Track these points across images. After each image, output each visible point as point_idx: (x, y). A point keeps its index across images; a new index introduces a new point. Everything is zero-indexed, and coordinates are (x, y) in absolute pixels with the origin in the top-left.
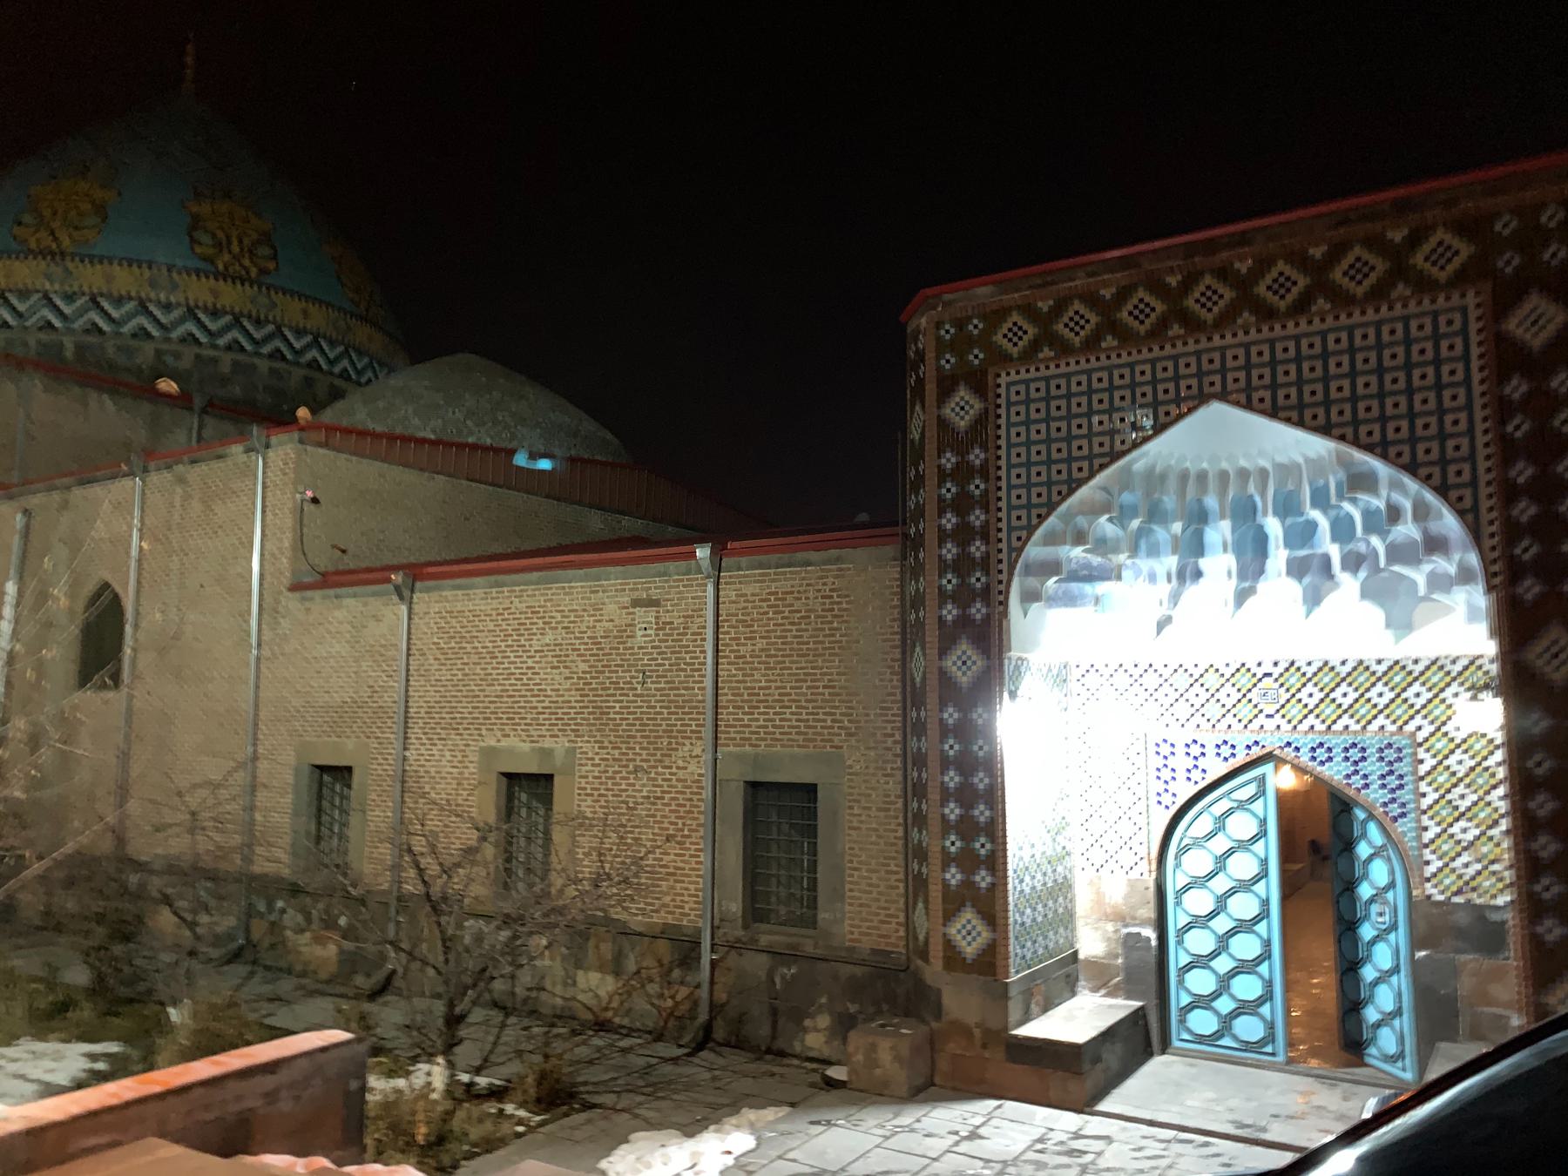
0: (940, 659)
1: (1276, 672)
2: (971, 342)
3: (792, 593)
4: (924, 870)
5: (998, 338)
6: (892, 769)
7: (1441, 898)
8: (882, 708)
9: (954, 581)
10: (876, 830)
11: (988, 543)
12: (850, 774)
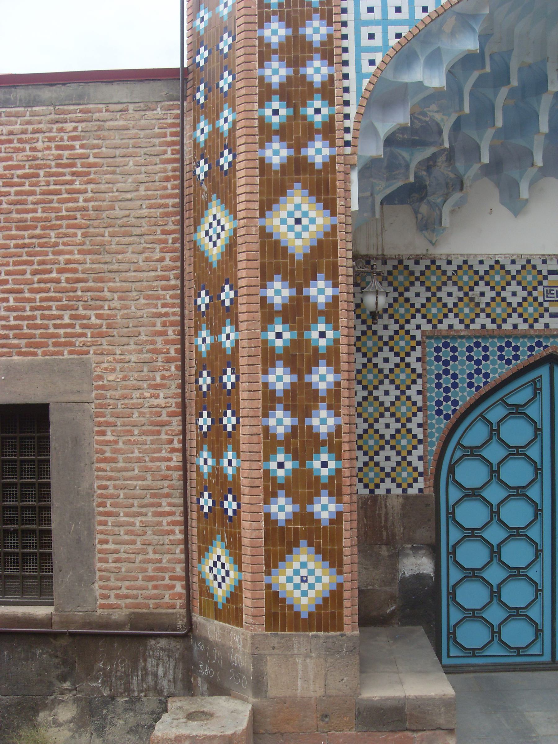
0: (262, 215)
3: (10, 141)
4: (230, 505)
8: (147, 297)
9: (283, 112)
10: (139, 460)
11: (331, 63)
12: (98, 388)
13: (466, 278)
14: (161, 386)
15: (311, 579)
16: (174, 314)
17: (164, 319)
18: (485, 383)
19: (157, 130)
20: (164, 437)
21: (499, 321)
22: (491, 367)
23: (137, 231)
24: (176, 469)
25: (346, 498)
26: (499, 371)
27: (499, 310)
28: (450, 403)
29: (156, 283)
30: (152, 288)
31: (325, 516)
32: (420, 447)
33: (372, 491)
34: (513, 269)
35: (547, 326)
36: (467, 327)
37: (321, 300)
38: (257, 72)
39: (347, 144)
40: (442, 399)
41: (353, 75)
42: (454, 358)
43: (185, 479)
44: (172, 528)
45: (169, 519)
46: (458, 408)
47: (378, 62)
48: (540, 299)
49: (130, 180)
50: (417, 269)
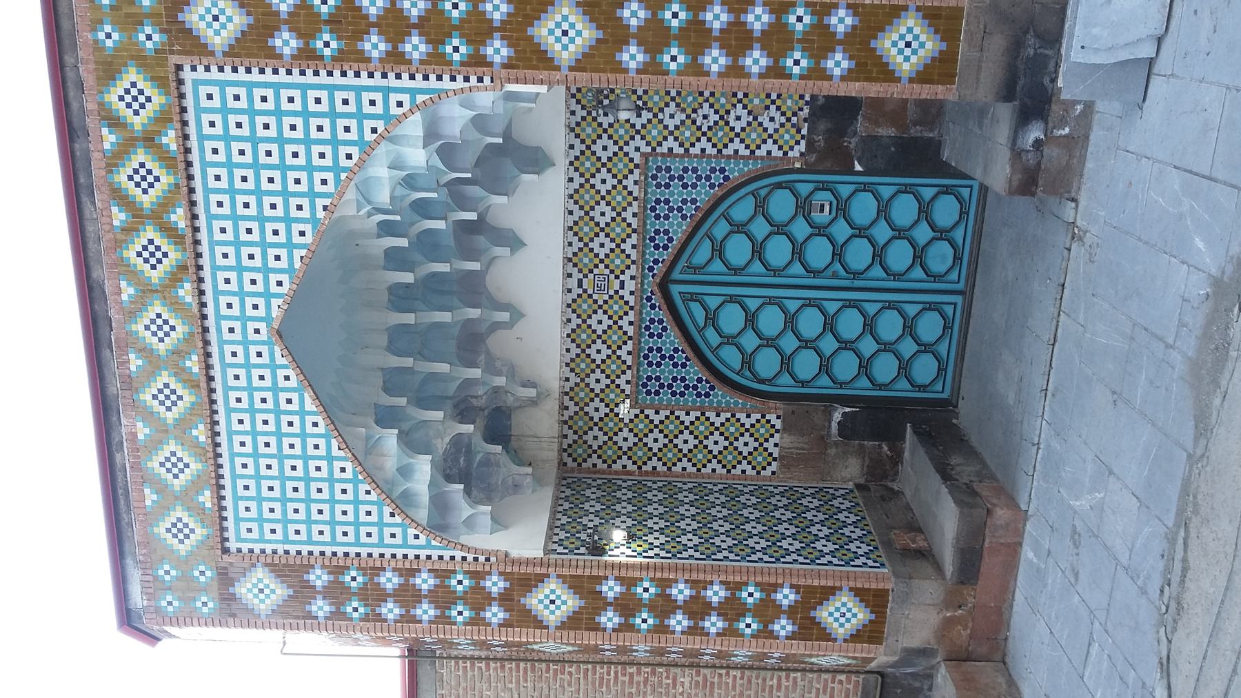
1: (577, 275)
2: (186, 578)
5: (183, 549)
6: (667, 678)
7: (803, 143)
8: (601, 685)
9: (460, 608)
11: (419, 571)
13: (583, 366)
14: (675, 680)
15: (843, 610)
16: (616, 668)
17: (619, 674)
18: (683, 352)
19: (461, 673)
20: (716, 680)
21: (625, 338)
22: (668, 345)
23: (546, 691)
24: (743, 674)
25: (780, 581)
26: (672, 338)
27: (615, 338)
28: (699, 385)
29: (590, 679)
30: (594, 683)
31: (792, 597)
32: (738, 415)
33: (775, 459)
34: (576, 321)
35: (632, 293)
36: (629, 367)
37: (617, 589)
38: (426, 625)
39: (488, 560)
40: (695, 392)
41: (428, 552)
42: (658, 378)
43: (751, 668)
44: (791, 679)
45: (783, 680)
46: (704, 378)
47: (417, 532)
48: (606, 297)
49: (503, 694)
50: (573, 408)
